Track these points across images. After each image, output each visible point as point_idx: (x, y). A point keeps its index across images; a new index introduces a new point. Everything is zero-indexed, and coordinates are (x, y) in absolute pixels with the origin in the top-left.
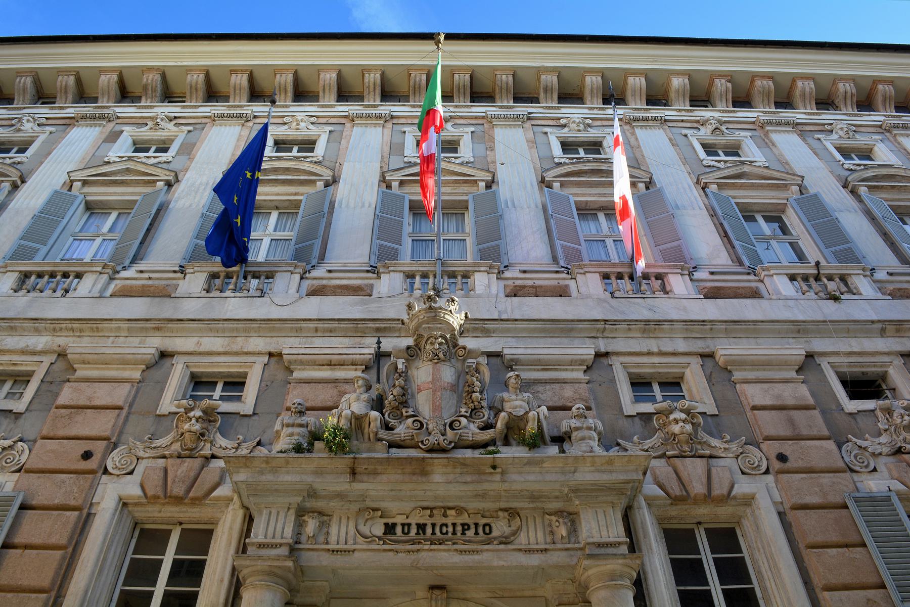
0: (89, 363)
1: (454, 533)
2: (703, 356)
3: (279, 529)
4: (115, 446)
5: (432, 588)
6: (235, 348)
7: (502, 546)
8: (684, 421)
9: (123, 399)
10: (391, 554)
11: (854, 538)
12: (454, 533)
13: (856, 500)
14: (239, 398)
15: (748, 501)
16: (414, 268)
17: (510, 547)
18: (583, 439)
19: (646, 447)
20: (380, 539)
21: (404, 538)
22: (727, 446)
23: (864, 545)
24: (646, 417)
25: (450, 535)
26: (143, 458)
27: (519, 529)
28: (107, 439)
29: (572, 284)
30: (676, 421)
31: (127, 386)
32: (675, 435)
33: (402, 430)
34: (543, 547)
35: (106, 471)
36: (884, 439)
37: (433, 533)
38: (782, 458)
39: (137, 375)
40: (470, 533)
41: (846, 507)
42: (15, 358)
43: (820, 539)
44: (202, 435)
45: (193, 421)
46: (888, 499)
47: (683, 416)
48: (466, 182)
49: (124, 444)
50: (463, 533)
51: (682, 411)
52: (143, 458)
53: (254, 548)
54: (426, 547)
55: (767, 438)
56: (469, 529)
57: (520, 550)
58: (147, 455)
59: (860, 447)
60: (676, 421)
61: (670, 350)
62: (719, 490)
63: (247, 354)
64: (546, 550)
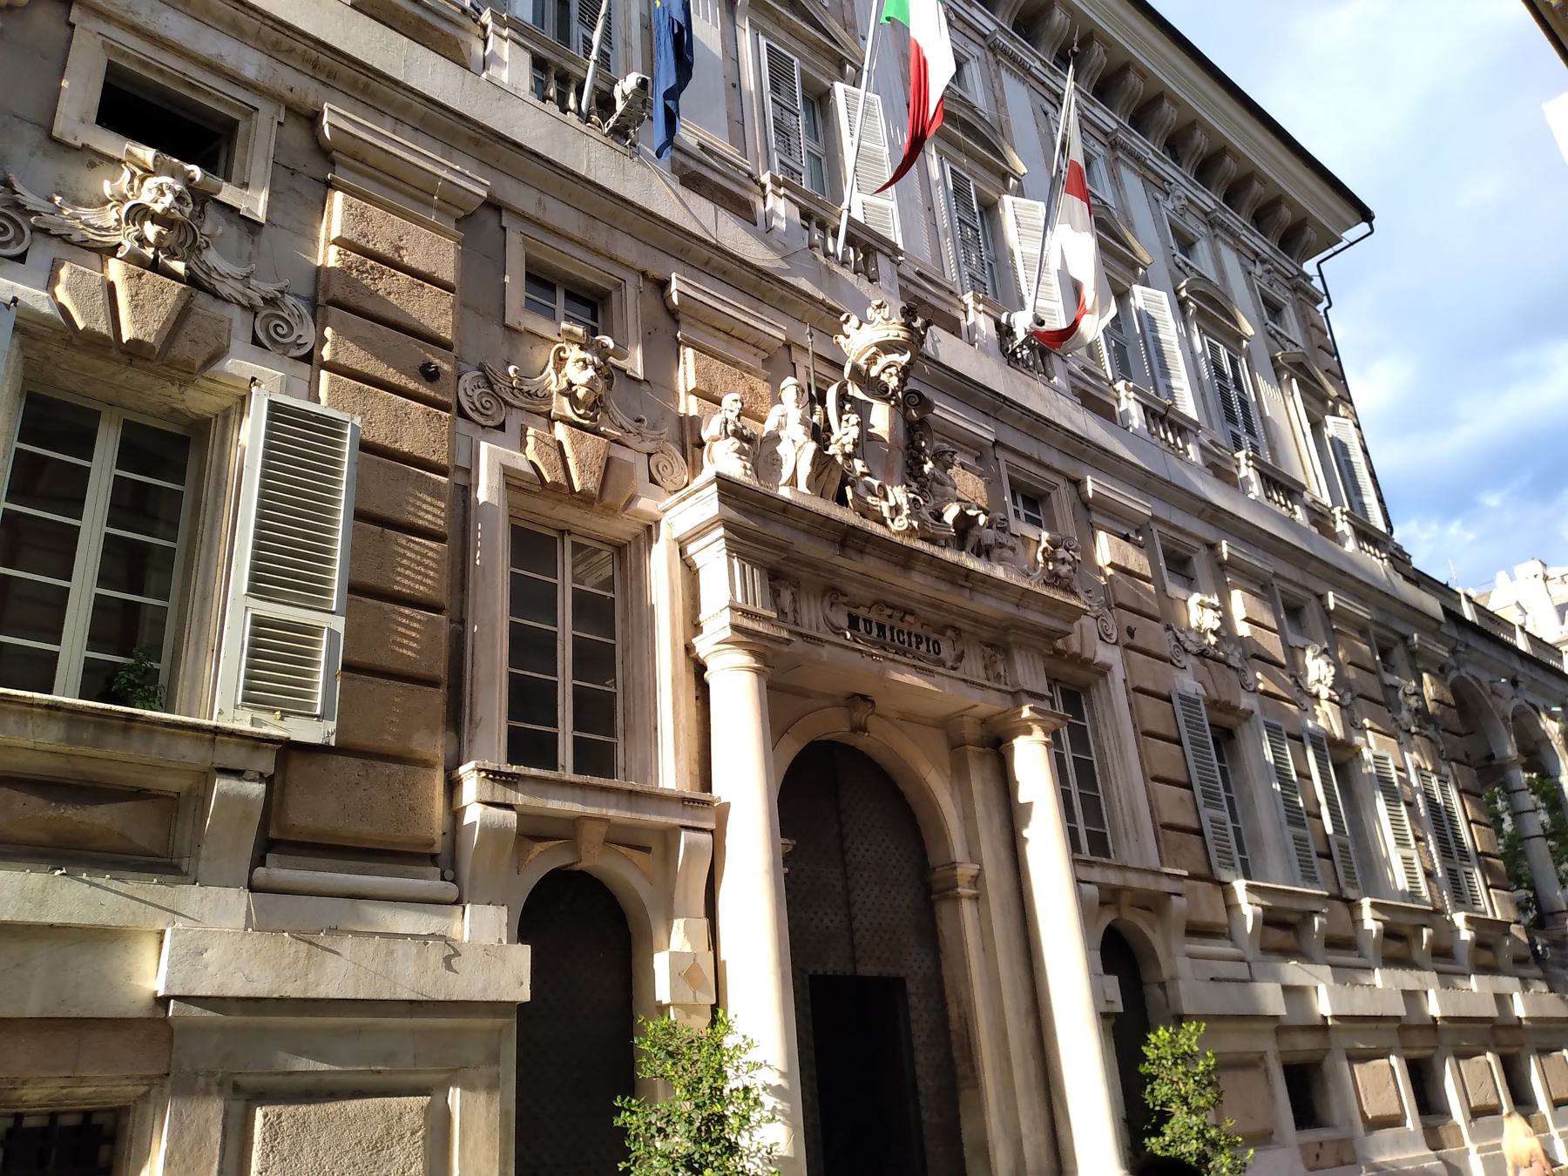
0: (363, 162)
7: (952, 673)
11: (1174, 735)
13: (1181, 697)
15: (1104, 670)
23: (1179, 742)
26: (512, 406)
35: (462, 413)
40: (923, 647)
41: (1169, 699)
42: (196, 74)
46: (1197, 702)
48: (829, 51)
55: (1120, 606)
57: (965, 681)
59: (1178, 639)
62: (1088, 655)
63: (612, 259)
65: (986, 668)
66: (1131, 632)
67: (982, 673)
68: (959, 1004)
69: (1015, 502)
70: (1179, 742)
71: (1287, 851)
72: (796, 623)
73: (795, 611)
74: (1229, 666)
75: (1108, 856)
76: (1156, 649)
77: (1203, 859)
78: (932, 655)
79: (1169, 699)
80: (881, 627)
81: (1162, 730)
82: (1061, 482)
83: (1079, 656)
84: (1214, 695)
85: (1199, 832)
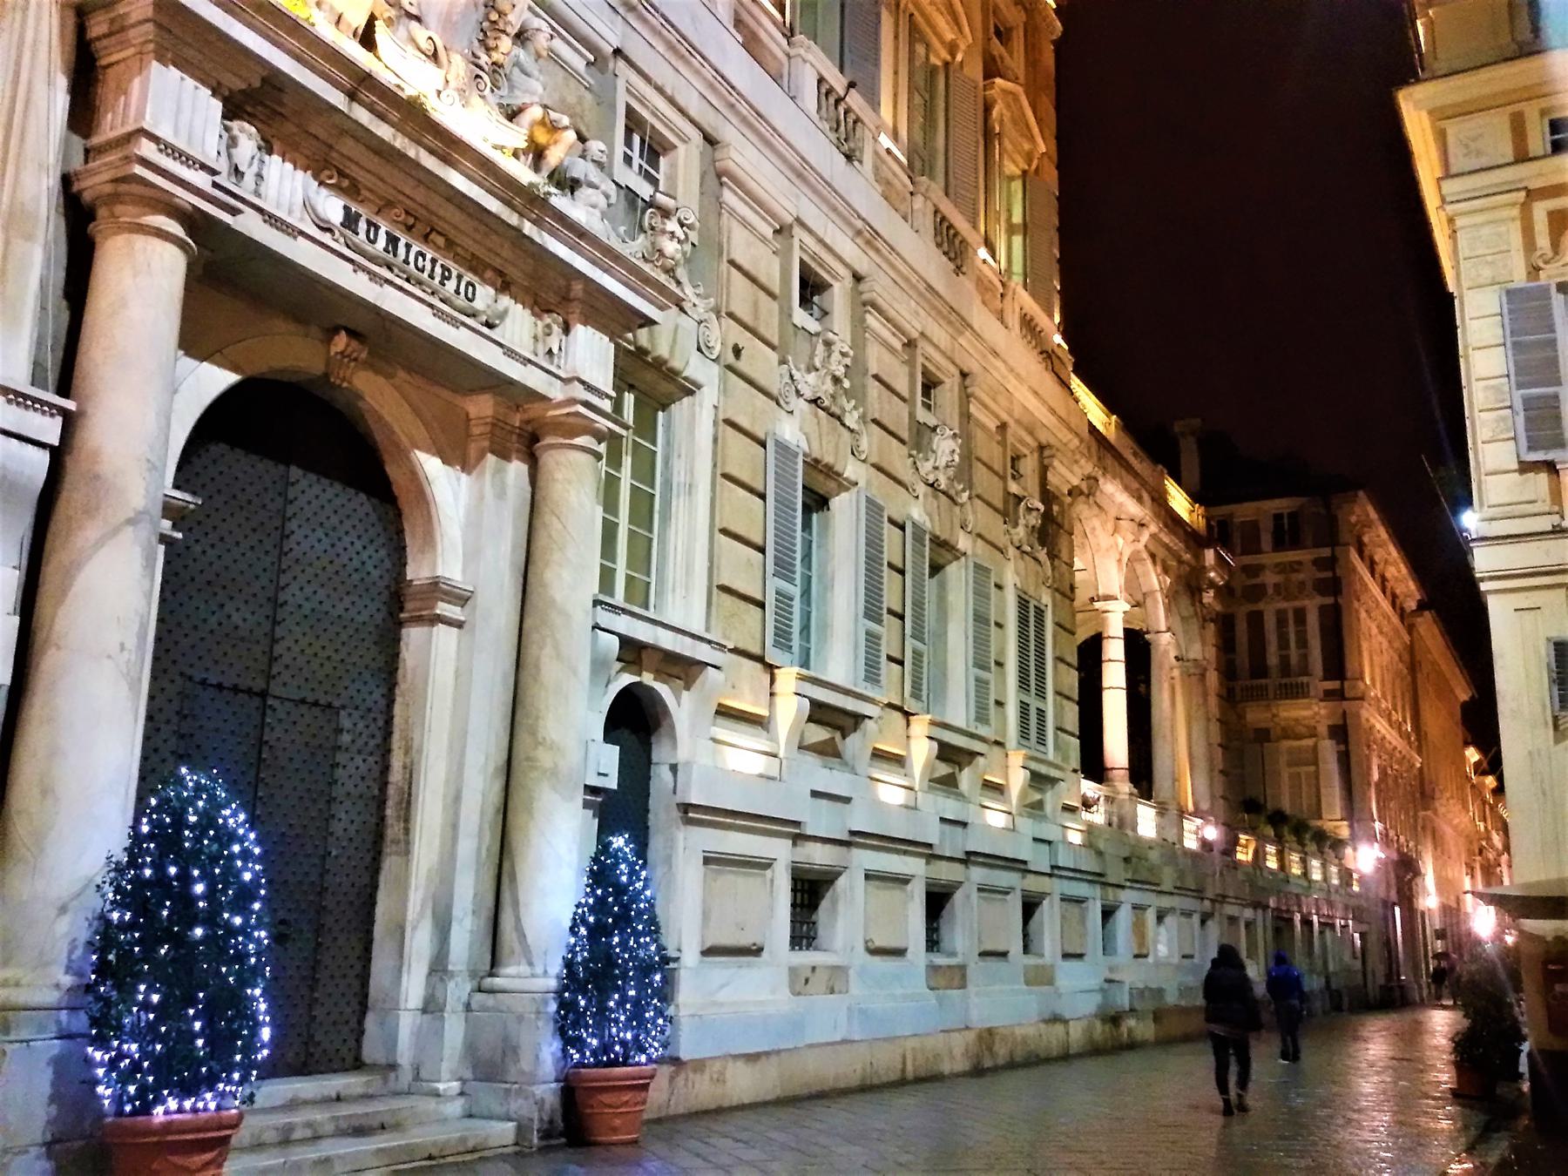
1: (431, 277)
7: (485, 330)
10: (350, 267)
11: (759, 487)
12: (431, 277)
13: (778, 443)
18: (594, 207)
23: (763, 497)
36: (811, 378)
37: (406, 262)
38: (737, 351)
40: (451, 285)
41: (763, 445)
43: (735, 472)
47: (679, 233)
51: (682, 225)
53: (153, 146)
54: (398, 281)
55: (731, 315)
56: (449, 278)
57: (501, 345)
59: (791, 376)
64: (530, 361)
65: (535, 338)
66: (737, 351)
67: (529, 342)
68: (407, 751)
69: (628, 143)
70: (763, 497)
71: (856, 647)
72: (257, 194)
73: (259, 176)
74: (844, 425)
75: (647, 608)
76: (762, 382)
77: (758, 636)
78: (461, 301)
79: (763, 445)
80: (393, 240)
81: (744, 476)
82: (696, 136)
83: (665, 362)
84: (816, 454)
85: (762, 605)
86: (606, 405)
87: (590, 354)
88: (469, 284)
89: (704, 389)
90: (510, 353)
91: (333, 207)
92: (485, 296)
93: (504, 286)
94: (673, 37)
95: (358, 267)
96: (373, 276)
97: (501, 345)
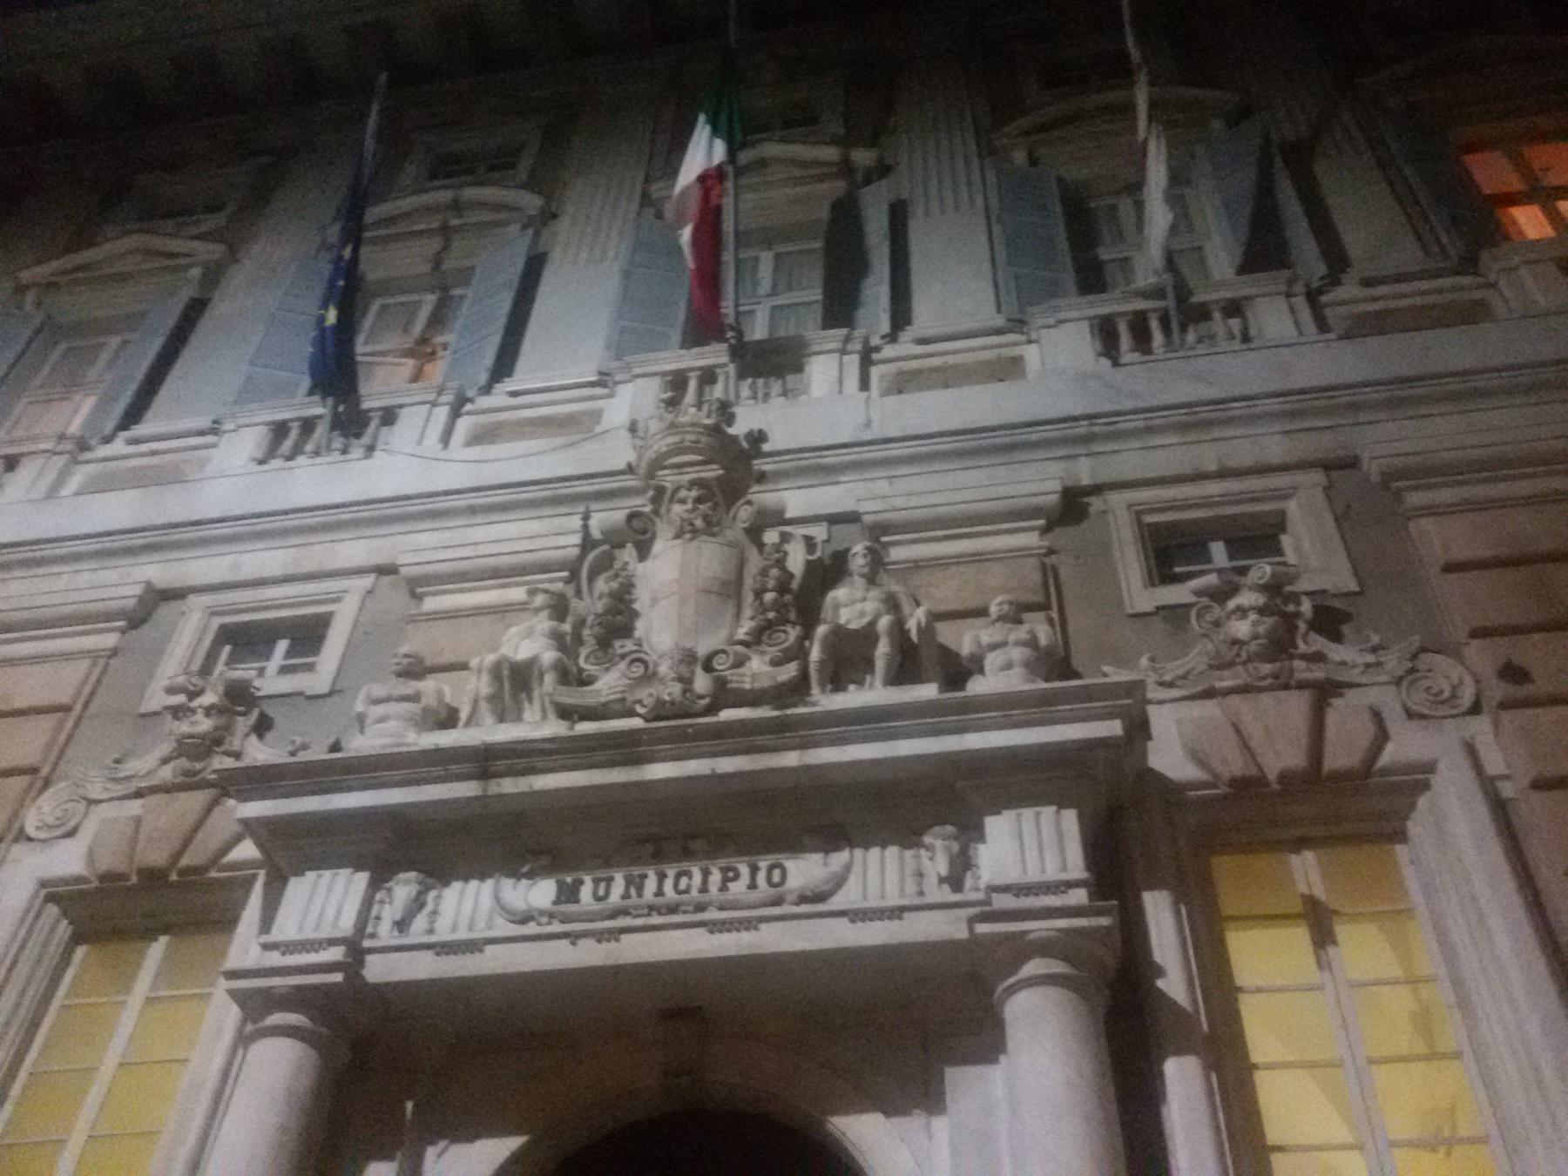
1: (704, 889)
2: (1328, 466)
3: (331, 912)
4: (47, 783)
5: (674, 1014)
6: (308, 566)
7: (805, 908)
8: (1261, 611)
9: (71, 691)
10: (565, 942)
12: (704, 889)
14: (310, 668)
16: (683, 365)
17: (821, 907)
19: (1168, 678)
20: (542, 913)
21: (597, 906)
22: (1370, 658)
24: (1174, 615)
25: (694, 893)
27: (848, 868)
28: (33, 771)
29: (1031, 354)
30: (1242, 612)
31: (85, 665)
32: (1236, 642)
33: (609, 683)
34: (894, 901)
37: (659, 893)
39: (110, 640)
40: (738, 888)
44: (219, 742)
45: (200, 716)
49: (67, 778)
50: (723, 888)
52: (101, 801)
54: (639, 922)
56: (737, 877)
57: (842, 914)
58: (106, 796)
60: (1242, 612)
61: (1247, 461)
80: (635, 883)
86: (1079, 897)
87: (1029, 849)
88: (771, 869)
89: (1441, 766)
90: (858, 915)
91: (542, 893)
92: (804, 870)
93: (833, 837)
94: (1178, 417)
95: (573, 937)
96: (600, 936)
97: (842, 914)
